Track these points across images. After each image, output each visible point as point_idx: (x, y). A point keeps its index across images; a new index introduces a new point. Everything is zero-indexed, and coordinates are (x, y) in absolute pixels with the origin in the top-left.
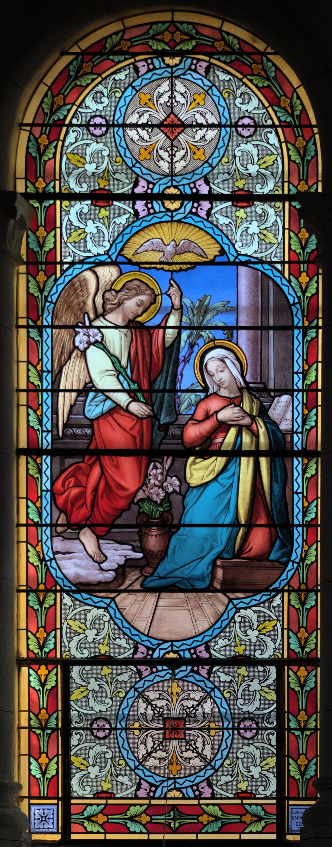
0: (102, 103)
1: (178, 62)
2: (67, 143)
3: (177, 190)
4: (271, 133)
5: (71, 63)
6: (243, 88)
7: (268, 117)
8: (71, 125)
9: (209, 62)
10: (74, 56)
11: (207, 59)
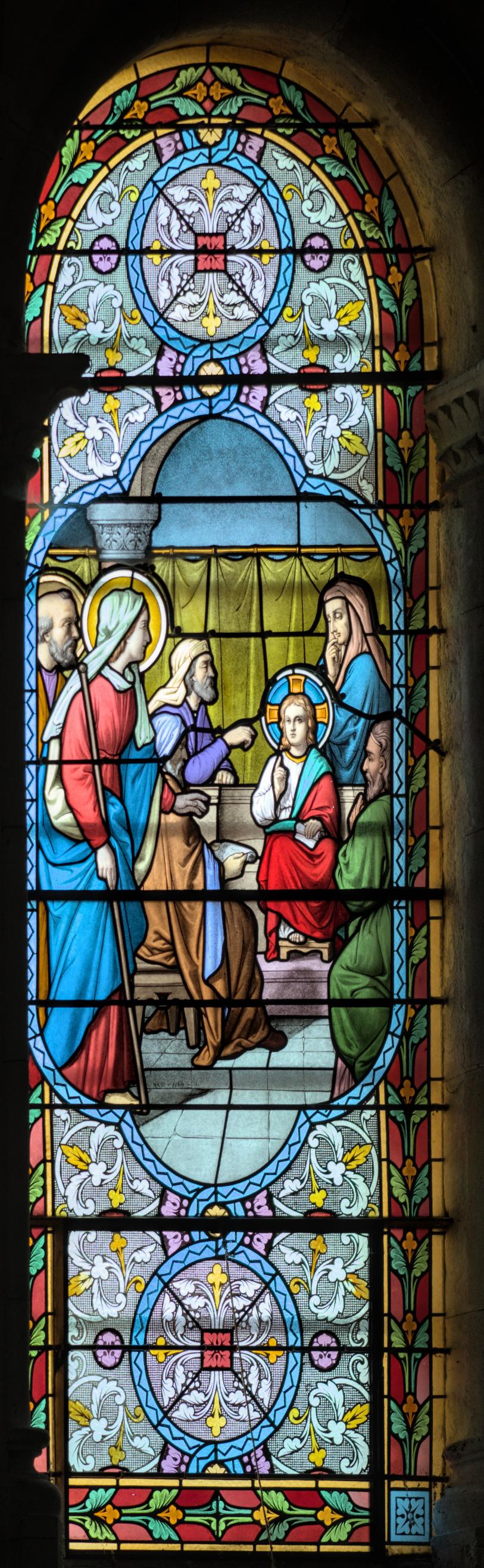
2: (59, 288)
6: (314, 184)
7: (349, 234)
9: (261, 136)
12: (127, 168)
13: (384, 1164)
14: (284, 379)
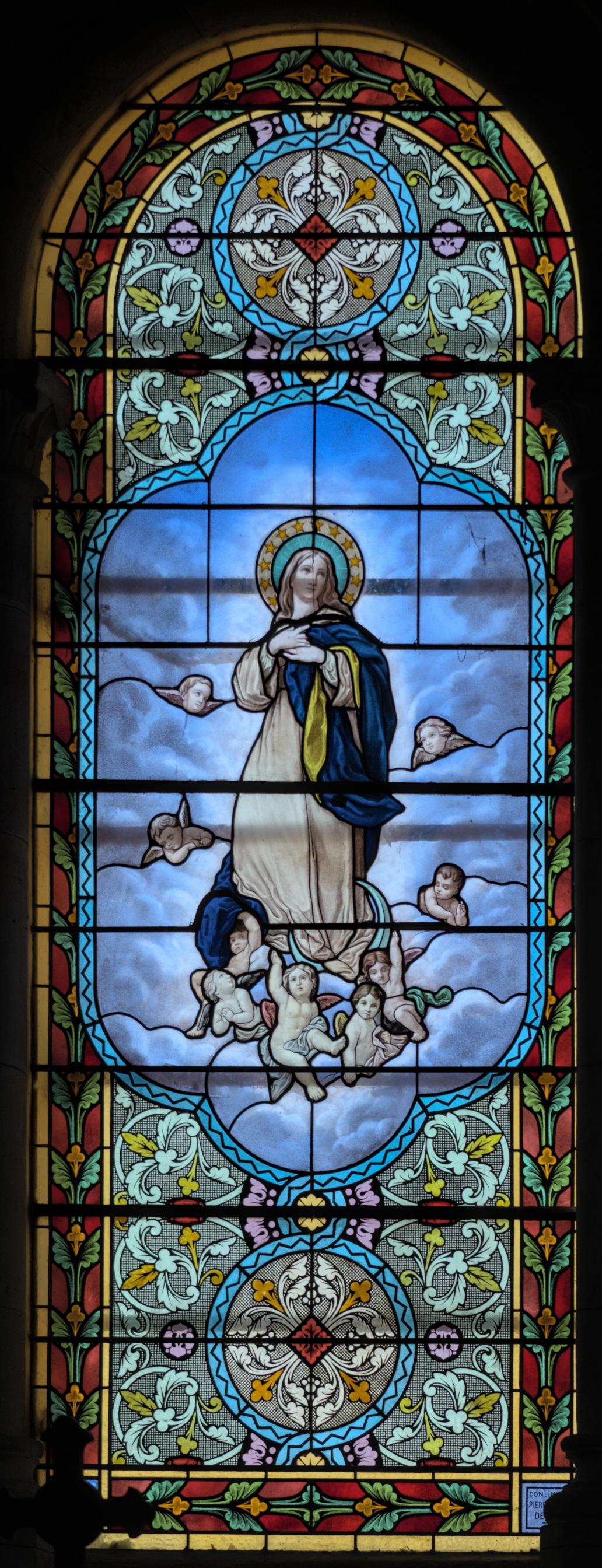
0: (191, 195)
2: (127, 269)
4: (493, 250)
6: (444, 169)
8: (135, 235)
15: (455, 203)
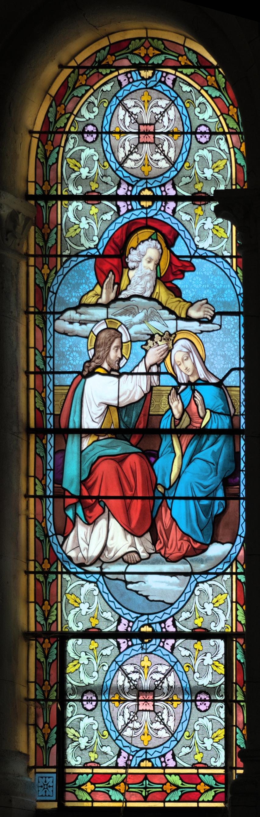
0: (94, 112)
1: (151, 75)
2: (67, 149)
3: (150, 192)
4: (222, 139)
5: (69, 76)
6: (201, 99)
7: (220, 125)
8: (70, 132)
9: (175, 75)
10: (72, 70)
11: (173, 72)
12: (102, 90)
13: (234, 604)
14: (184, 198)
15: (206, 116)
